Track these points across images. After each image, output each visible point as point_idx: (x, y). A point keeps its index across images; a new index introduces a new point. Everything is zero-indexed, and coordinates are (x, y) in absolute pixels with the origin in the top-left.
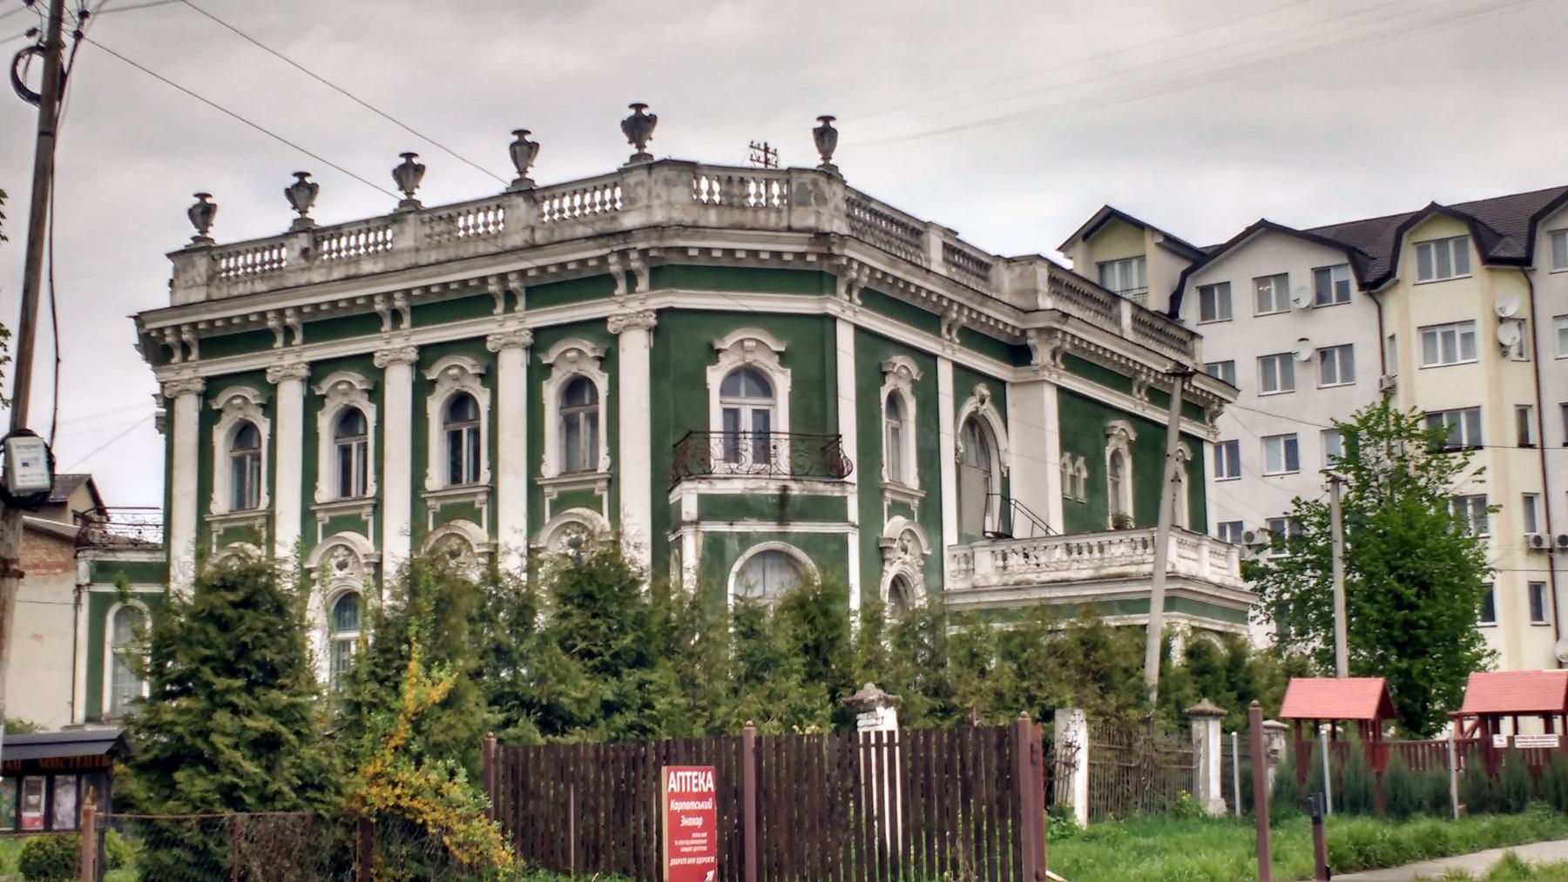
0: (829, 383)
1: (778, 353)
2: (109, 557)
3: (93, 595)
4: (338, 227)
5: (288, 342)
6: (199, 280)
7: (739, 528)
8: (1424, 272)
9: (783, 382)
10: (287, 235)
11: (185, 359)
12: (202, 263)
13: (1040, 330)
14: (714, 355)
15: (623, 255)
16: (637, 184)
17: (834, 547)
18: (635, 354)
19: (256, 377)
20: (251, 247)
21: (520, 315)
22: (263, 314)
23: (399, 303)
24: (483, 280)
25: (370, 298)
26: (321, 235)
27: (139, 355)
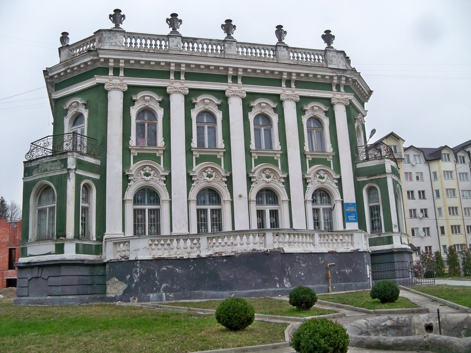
2: (81, 158)
3: (77, 176)
6: (118, 44)
10: (168, 36)
15: (339, 78)
16: (333, 56)
22: (168, 64)
24: (281, 73)
26: (184, 39)
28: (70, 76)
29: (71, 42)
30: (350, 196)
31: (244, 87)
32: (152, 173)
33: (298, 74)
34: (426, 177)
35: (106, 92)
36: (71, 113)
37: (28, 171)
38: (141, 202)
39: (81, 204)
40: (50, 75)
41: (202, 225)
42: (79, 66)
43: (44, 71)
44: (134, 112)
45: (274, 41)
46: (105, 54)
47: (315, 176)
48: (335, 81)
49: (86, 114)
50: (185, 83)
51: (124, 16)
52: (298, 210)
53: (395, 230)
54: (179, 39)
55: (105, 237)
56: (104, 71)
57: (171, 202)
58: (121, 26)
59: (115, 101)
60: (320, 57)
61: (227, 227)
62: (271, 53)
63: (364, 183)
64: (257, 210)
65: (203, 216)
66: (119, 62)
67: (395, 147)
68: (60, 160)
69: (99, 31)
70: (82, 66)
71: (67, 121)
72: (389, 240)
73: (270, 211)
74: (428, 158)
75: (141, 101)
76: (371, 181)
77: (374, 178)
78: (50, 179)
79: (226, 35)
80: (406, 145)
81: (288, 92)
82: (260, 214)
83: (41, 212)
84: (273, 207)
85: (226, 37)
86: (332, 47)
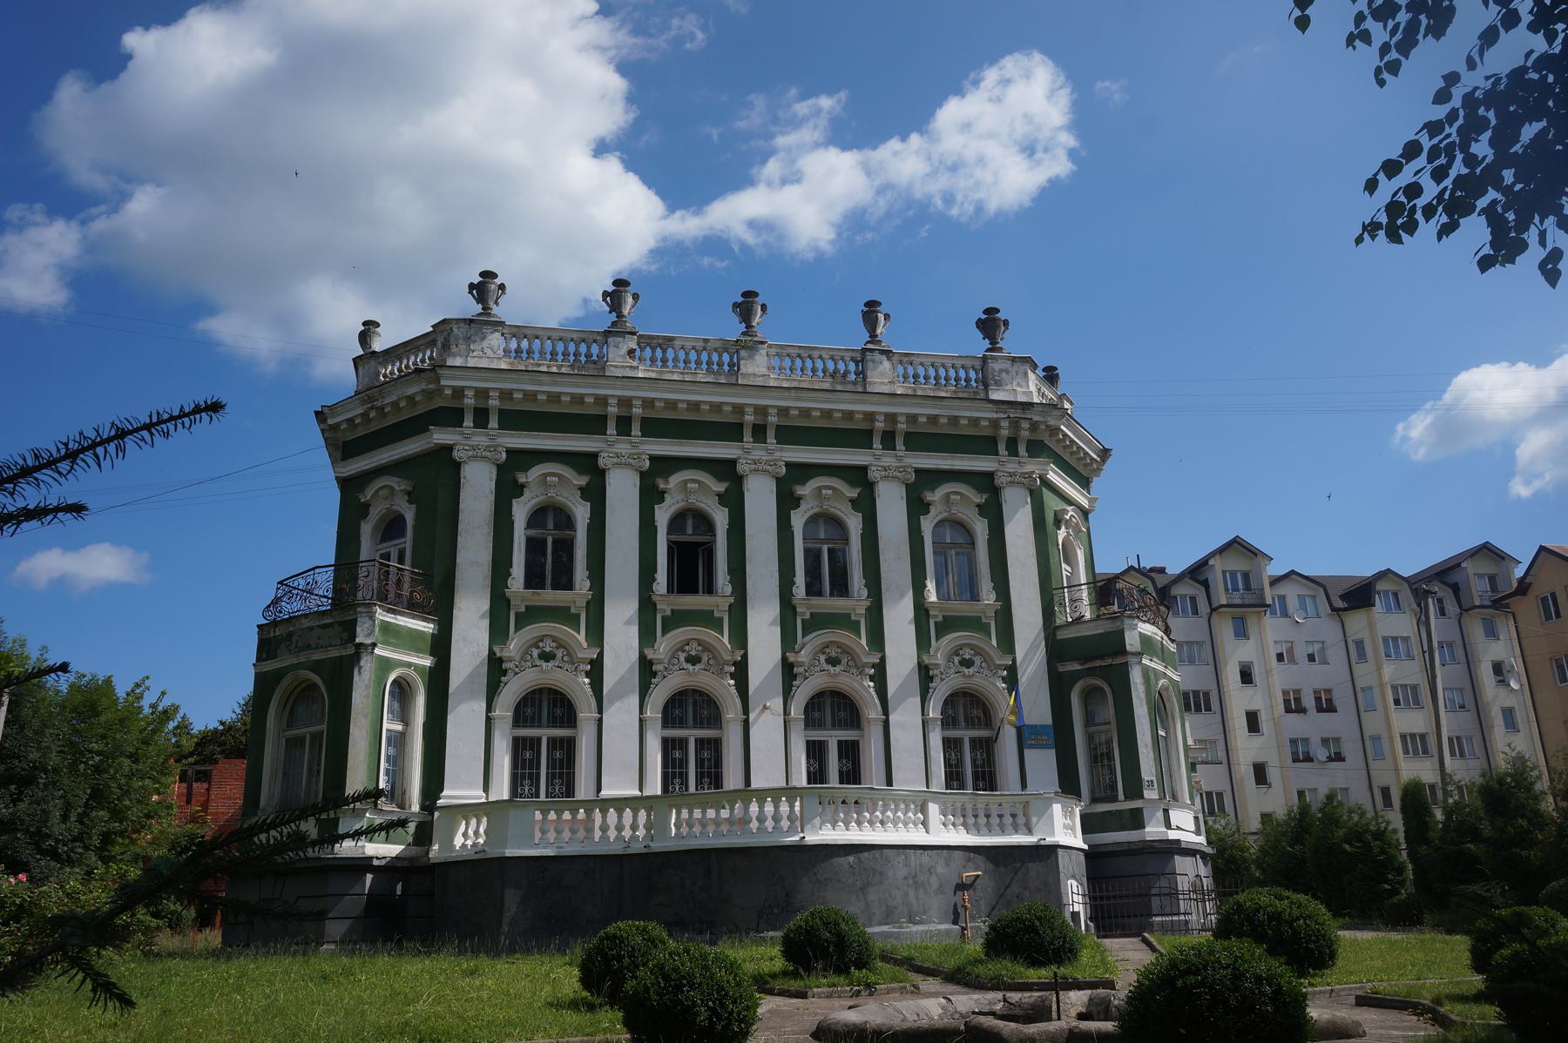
4: (671, 339)
7: (1153, 665)
10: (607, 334)
15: (1015, 424)
16: (1001, 371)
24: (870, 417)
28: (375, 427)
29: (378, 345)
30: (1039, 711)
32: (559, 654)
33: (912, 419)
34: (1336, 655)
35: (457, 466)
36: (375, 513)
37: (266, 648)
38: (534, 722)
39: (386, 726)
40: (330, 422)
41: (674, 777)
42: (395, 404)
43: (317, 413)
44: (520, 512)
45: (860, 338)
46: (453, 378)
47: (950, 660)
48: (1005, 433)
49: (410, 517)
50: (642, 443)
51: (502, 287)
53: (1151, 794)
55: (440, 802)
56: (452, 417)
57: (600, 721)
58: (495, 310)
59: (478, 484)
60: (972, 374)
61: (732, 779)
62: (852, 367)
63: (1075, 677)
64: (808, 742)
65: (677, 754)
66: (487, 397)
67: (1246, 576)
68: (341, 624)
69: (444, 321)
70: (402, 404)
71: (366, 529)
72: (1136, 820)
73: (840, 742)
74: (1340, 604)
75: (538, 484)
76: (1091, 672)
77: (1098, 663)
78: (316, 667)
79: (743, 327)
80: (1275, 569)
81: (888, 460)
82: (816, 751)
83: (294, 744)
84: (848, 735)
85: (744, 334)
86: (1000, 350)
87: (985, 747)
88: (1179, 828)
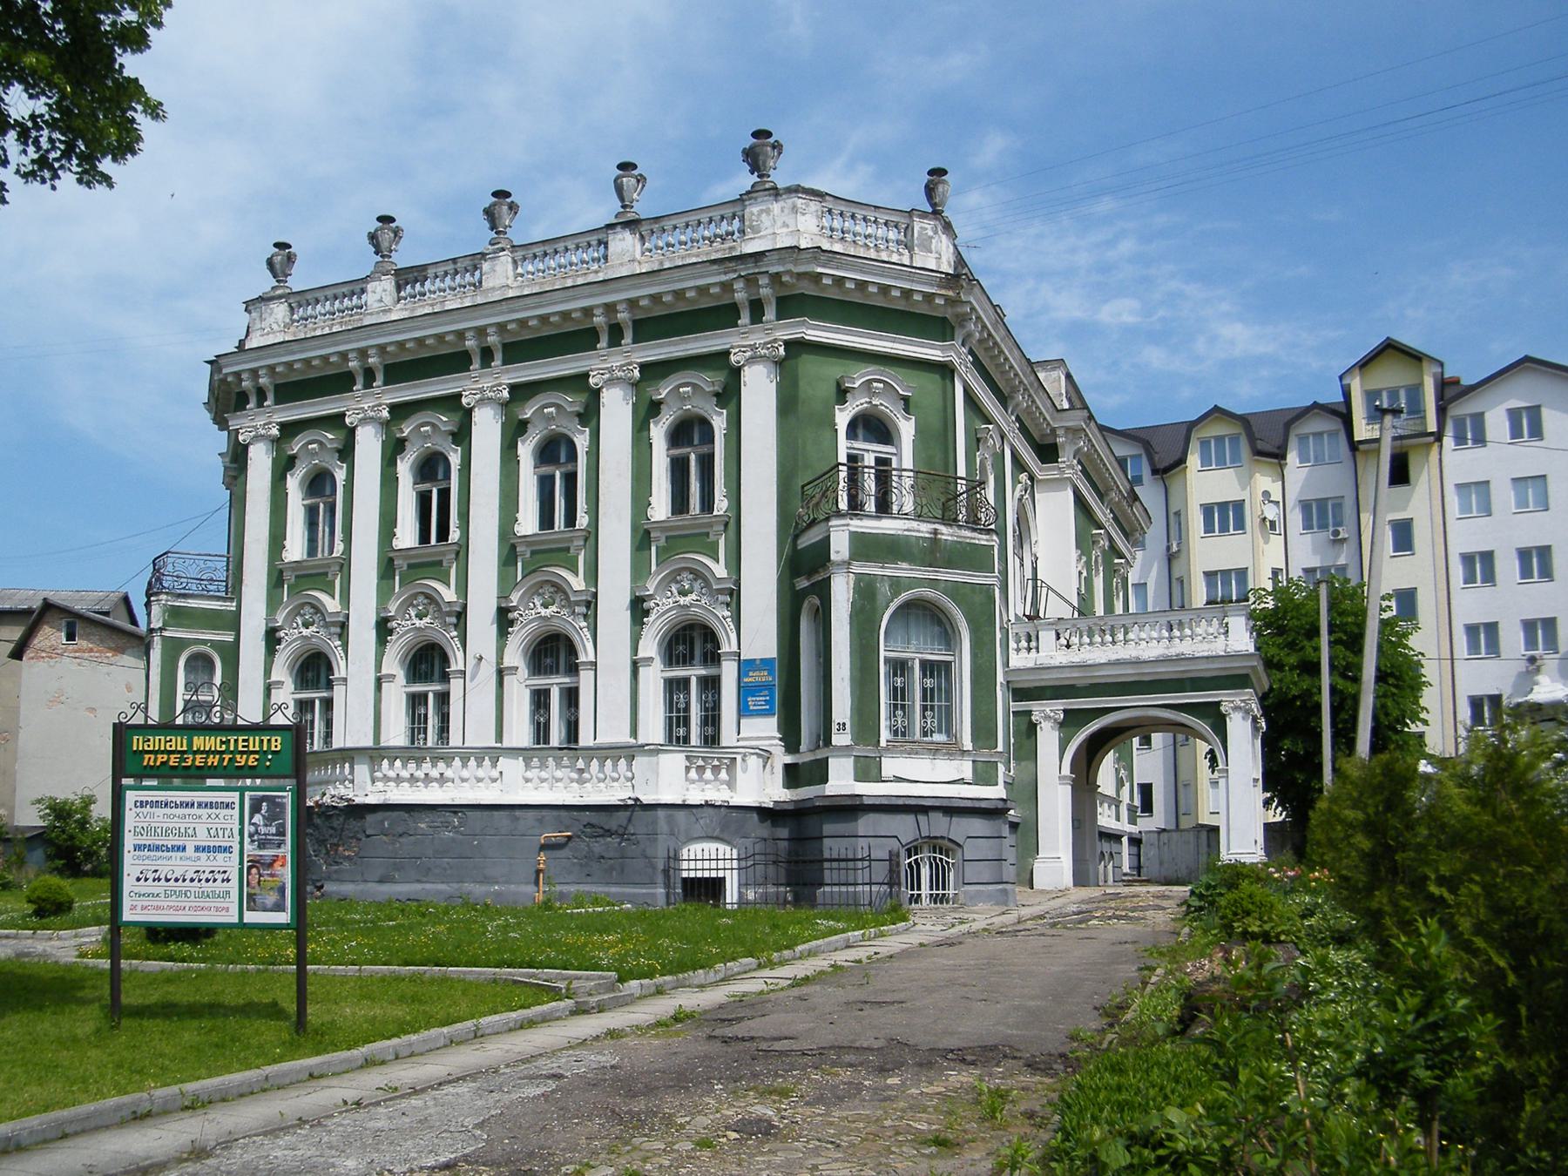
0: (950, 434)
1: (906, 399)
5: (368, 384)
6: (275, 327)
7: (888, 572)
8: (1205, 461)
9: (906, 429)
11: (260, 405)
12: (280, 311)
13: (1067, 429)
14: (842, 394)
17: (978, 599)
18: (759, 391)
19: (335, 421)
20: (329, 293)
21: (625, 349)
22: (344, 356)
23: (493, 339)
25: (460, 334)
27: (206, 417)
31: (508, 371)
52: (621, 683)
54: (387, 285)
72: (818, 772)
87: (711, 685)
88: (899, 780)
